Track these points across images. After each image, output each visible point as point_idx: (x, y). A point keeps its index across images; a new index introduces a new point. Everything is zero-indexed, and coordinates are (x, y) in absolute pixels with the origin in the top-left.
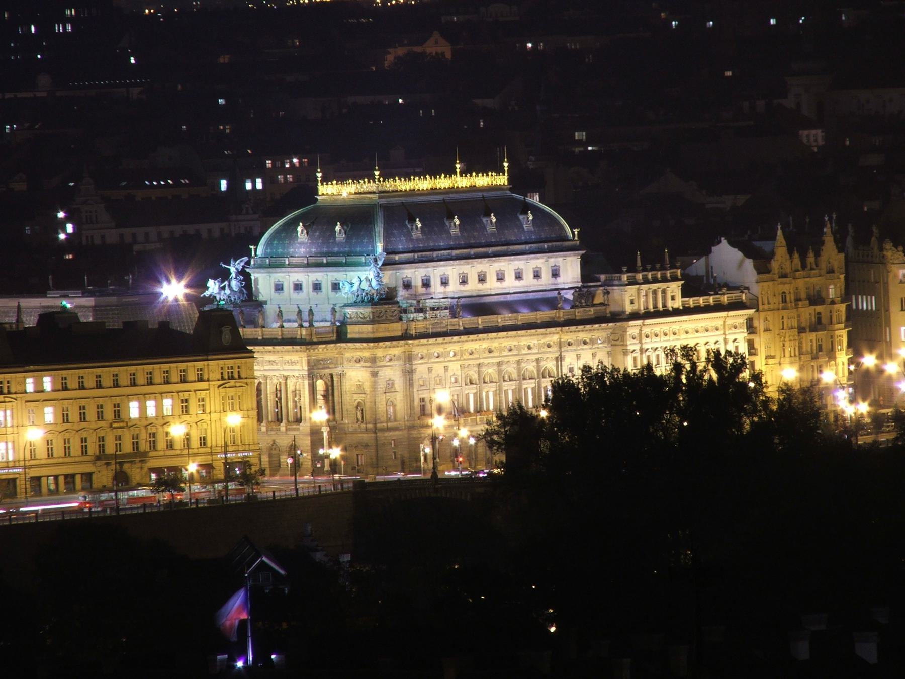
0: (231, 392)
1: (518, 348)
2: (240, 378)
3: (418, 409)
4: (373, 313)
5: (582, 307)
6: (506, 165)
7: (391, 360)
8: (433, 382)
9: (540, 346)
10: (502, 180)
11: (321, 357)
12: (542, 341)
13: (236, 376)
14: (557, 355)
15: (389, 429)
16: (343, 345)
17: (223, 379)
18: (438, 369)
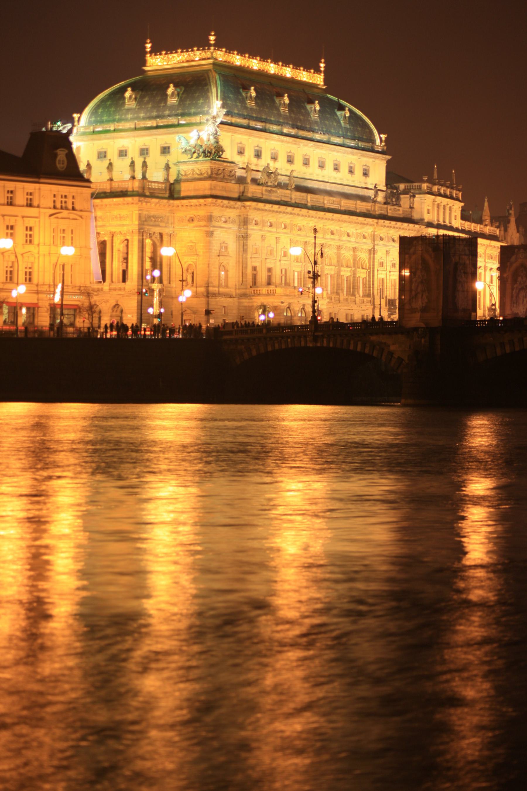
0: (63, 224)
1: (340, 234)
2: (73, 209)
3: (250, 277)
4: (212, 169)
5: (393, 205)
6: (322, 65)
7: (226, 222)
8: (265, 252)
9: (357, 236)
10: (319, 80)
11: (152, 213)
12: (359, 231)
13: (70, 206)
14: (371, 247)
15: (219, 294)
16: (177, 202)
17: (55, 207)
18: (271, 239)
